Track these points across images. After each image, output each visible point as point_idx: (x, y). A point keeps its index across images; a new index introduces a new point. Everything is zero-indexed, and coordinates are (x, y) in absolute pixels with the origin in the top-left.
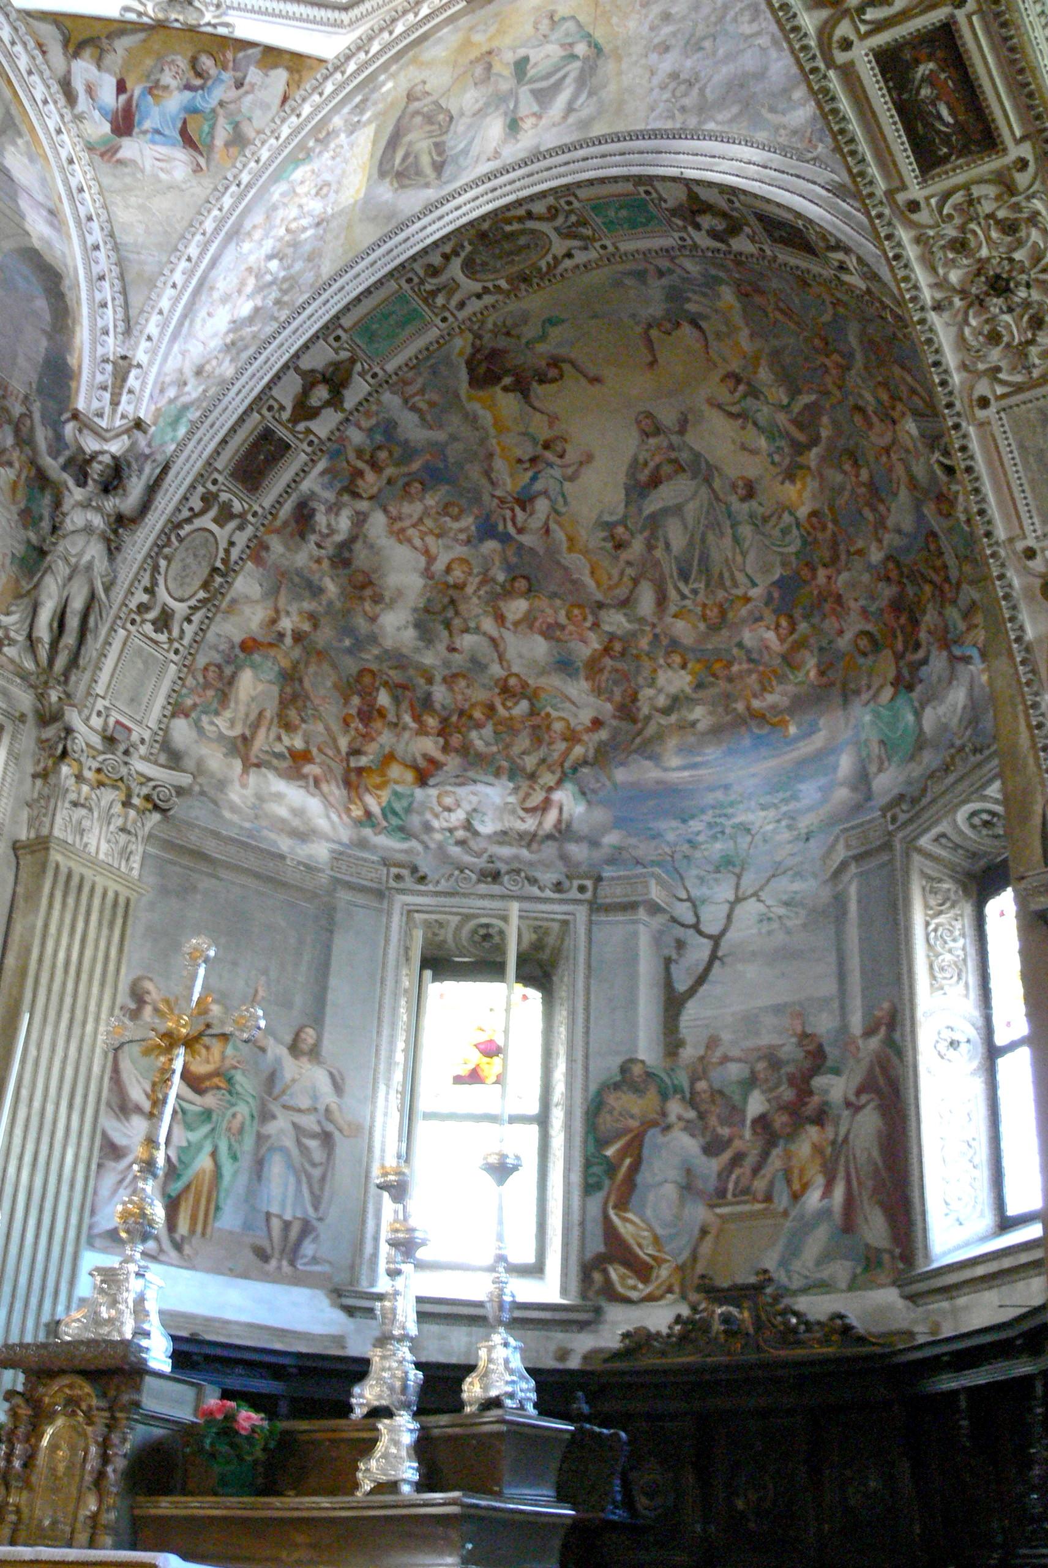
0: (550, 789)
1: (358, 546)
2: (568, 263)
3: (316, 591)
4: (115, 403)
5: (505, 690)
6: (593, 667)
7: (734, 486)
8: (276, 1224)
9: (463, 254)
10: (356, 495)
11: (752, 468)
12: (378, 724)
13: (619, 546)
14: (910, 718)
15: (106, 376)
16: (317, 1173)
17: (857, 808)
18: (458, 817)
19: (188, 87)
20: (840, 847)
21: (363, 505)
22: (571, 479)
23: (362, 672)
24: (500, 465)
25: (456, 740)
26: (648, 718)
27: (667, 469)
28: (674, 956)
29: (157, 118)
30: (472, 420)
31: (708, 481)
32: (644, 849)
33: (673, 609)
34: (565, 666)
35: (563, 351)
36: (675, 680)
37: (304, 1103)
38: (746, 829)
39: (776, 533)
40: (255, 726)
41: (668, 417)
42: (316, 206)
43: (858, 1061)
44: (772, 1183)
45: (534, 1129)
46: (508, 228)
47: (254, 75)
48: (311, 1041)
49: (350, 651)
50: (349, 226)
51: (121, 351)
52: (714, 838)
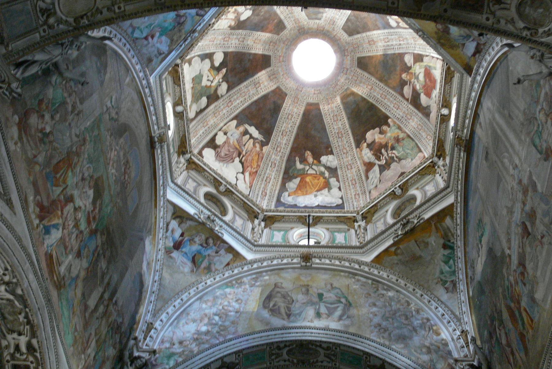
2: (320, 364)
4: (145, 339)
9: (291, 347)
15: (144, 328)
19: (201, 245)
29: (188, 249)
42: (236, 306)
46: (310, 346)
47: (222, 252)
51: (151, 321)
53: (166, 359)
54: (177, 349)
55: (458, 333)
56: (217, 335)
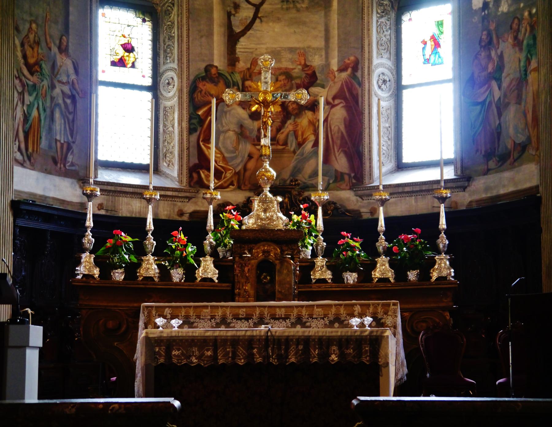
8: (58, 144)
16: (71, 117)
28: (233, 12)
37: (64, 79)
43: (334, 83)
44: (287, 136)
45: (148, 96)
48: (65, 44)
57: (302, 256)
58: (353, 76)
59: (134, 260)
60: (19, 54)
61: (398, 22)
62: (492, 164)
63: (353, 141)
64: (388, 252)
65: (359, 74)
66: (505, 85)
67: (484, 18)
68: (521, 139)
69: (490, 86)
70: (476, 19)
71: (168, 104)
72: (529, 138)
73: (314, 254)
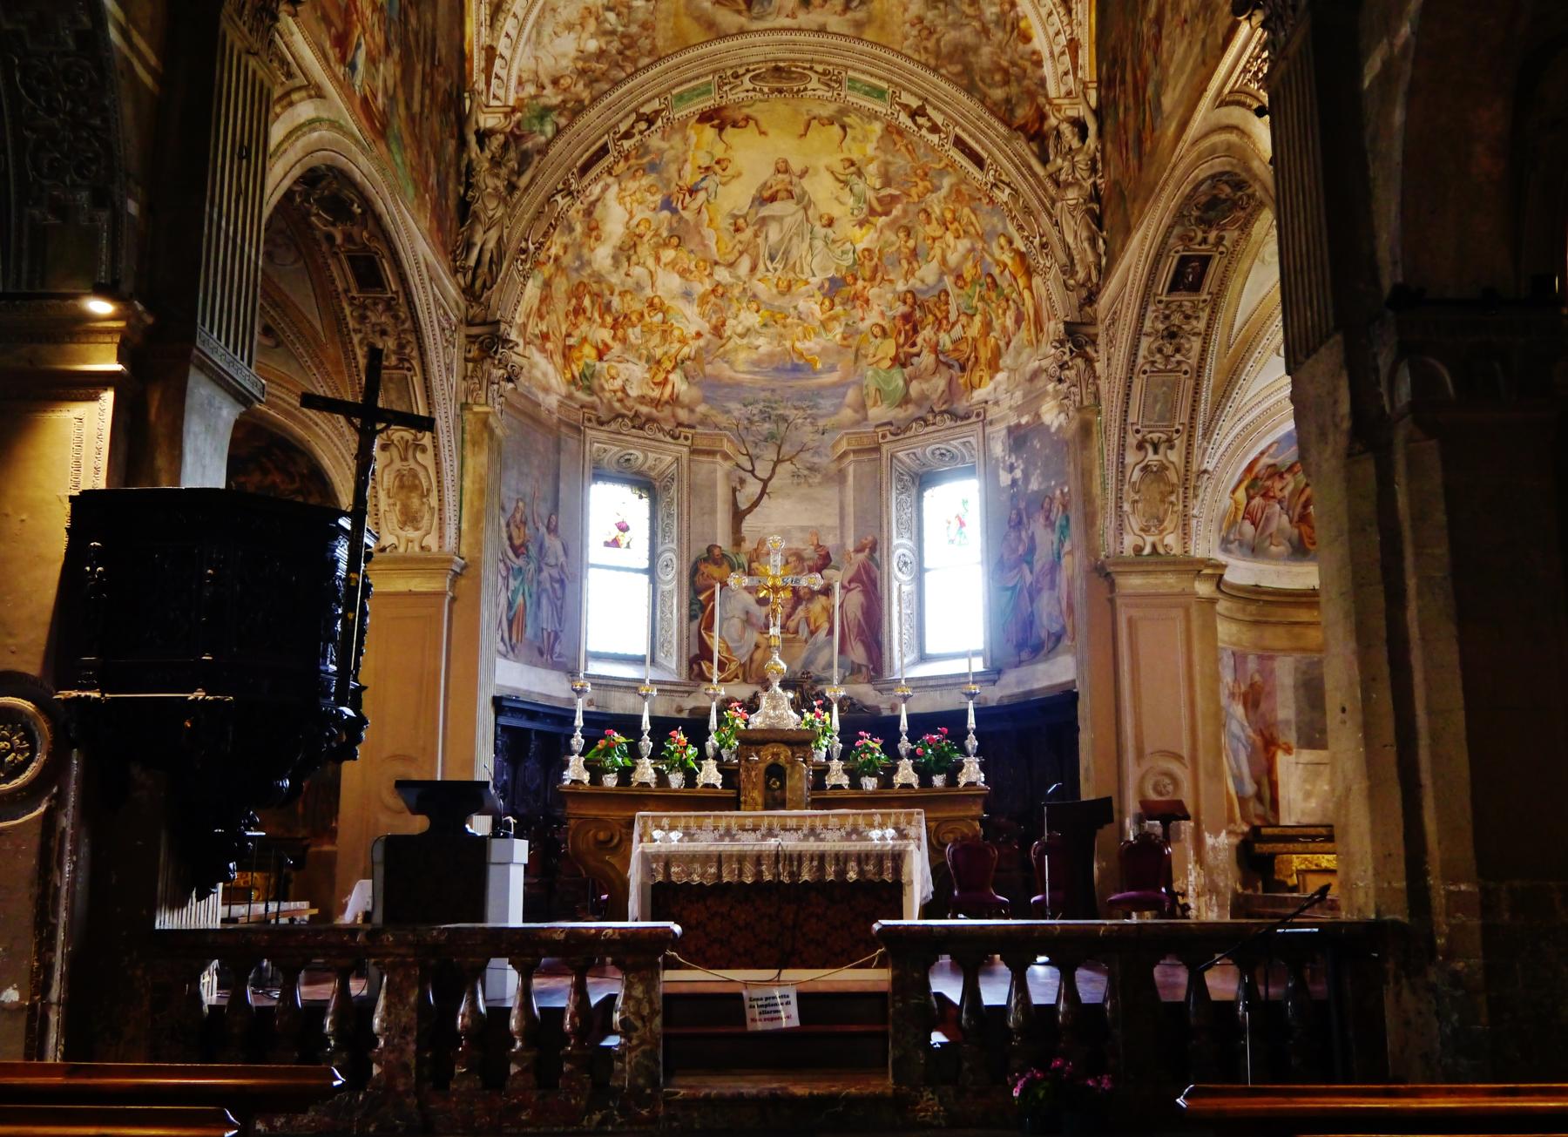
0: (668, 372)
1: (599, 204)
3: (571, 230)
4: (488, 83)
5: (651, 305)
6: (703, 300)
7: (821, 217)
10: (610, 174)
11: (836, 211)
12: (581, 318)
13: (737, 230)
14: (901, 383)
15: (483, 64)
17: (857, 423)
18: (618, 383)
20: (844, 443)
21: (610, 180)
22: (724, 184)
23: (581, 283)
24: (688, 168)
25: (620, 333)
26: (730, 338)
27: (783, 194)
30: (686, 139)
31: (805, 209)
32: (722, 419)
33: (759, 275)
34: (687, 295)
35: (754, 114)
36: (750, 319)
37: (552, 561)
38: (784, 419)
39: (839, 252)
40: (528, 316)
41: (796, 165)
49: (577, 270)
50: (676, 15)
52: (764, 420)
53: (535, 122)
54: (552, 97)
55: (1062, 40)
56: (620, 58)
57: (816, 758)
58: (871, 557)
59: (628, 763)
60: (505, 535)
61: (920, 498)
62: (1024, 655)
63: (870, 631)
64: (912, 755)
65: (877, 555)
66: (1037, 567)
67: (1013, 497)
68: (1056, 628)
69: (1021, 570)
70: (1004, 497)
71: (667, 588)
72: (1064, 628)
73: (829, 757)
